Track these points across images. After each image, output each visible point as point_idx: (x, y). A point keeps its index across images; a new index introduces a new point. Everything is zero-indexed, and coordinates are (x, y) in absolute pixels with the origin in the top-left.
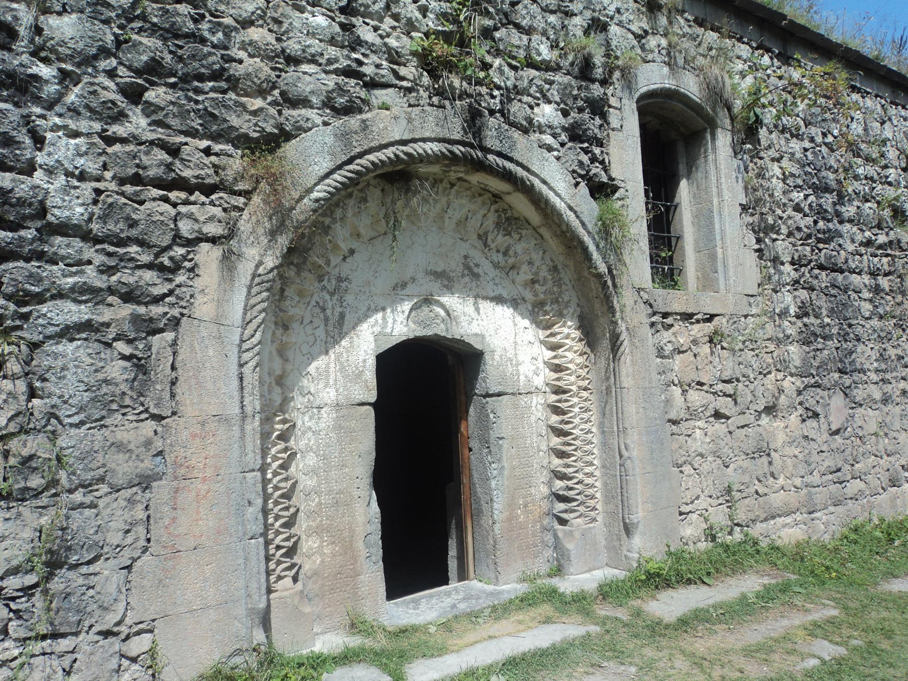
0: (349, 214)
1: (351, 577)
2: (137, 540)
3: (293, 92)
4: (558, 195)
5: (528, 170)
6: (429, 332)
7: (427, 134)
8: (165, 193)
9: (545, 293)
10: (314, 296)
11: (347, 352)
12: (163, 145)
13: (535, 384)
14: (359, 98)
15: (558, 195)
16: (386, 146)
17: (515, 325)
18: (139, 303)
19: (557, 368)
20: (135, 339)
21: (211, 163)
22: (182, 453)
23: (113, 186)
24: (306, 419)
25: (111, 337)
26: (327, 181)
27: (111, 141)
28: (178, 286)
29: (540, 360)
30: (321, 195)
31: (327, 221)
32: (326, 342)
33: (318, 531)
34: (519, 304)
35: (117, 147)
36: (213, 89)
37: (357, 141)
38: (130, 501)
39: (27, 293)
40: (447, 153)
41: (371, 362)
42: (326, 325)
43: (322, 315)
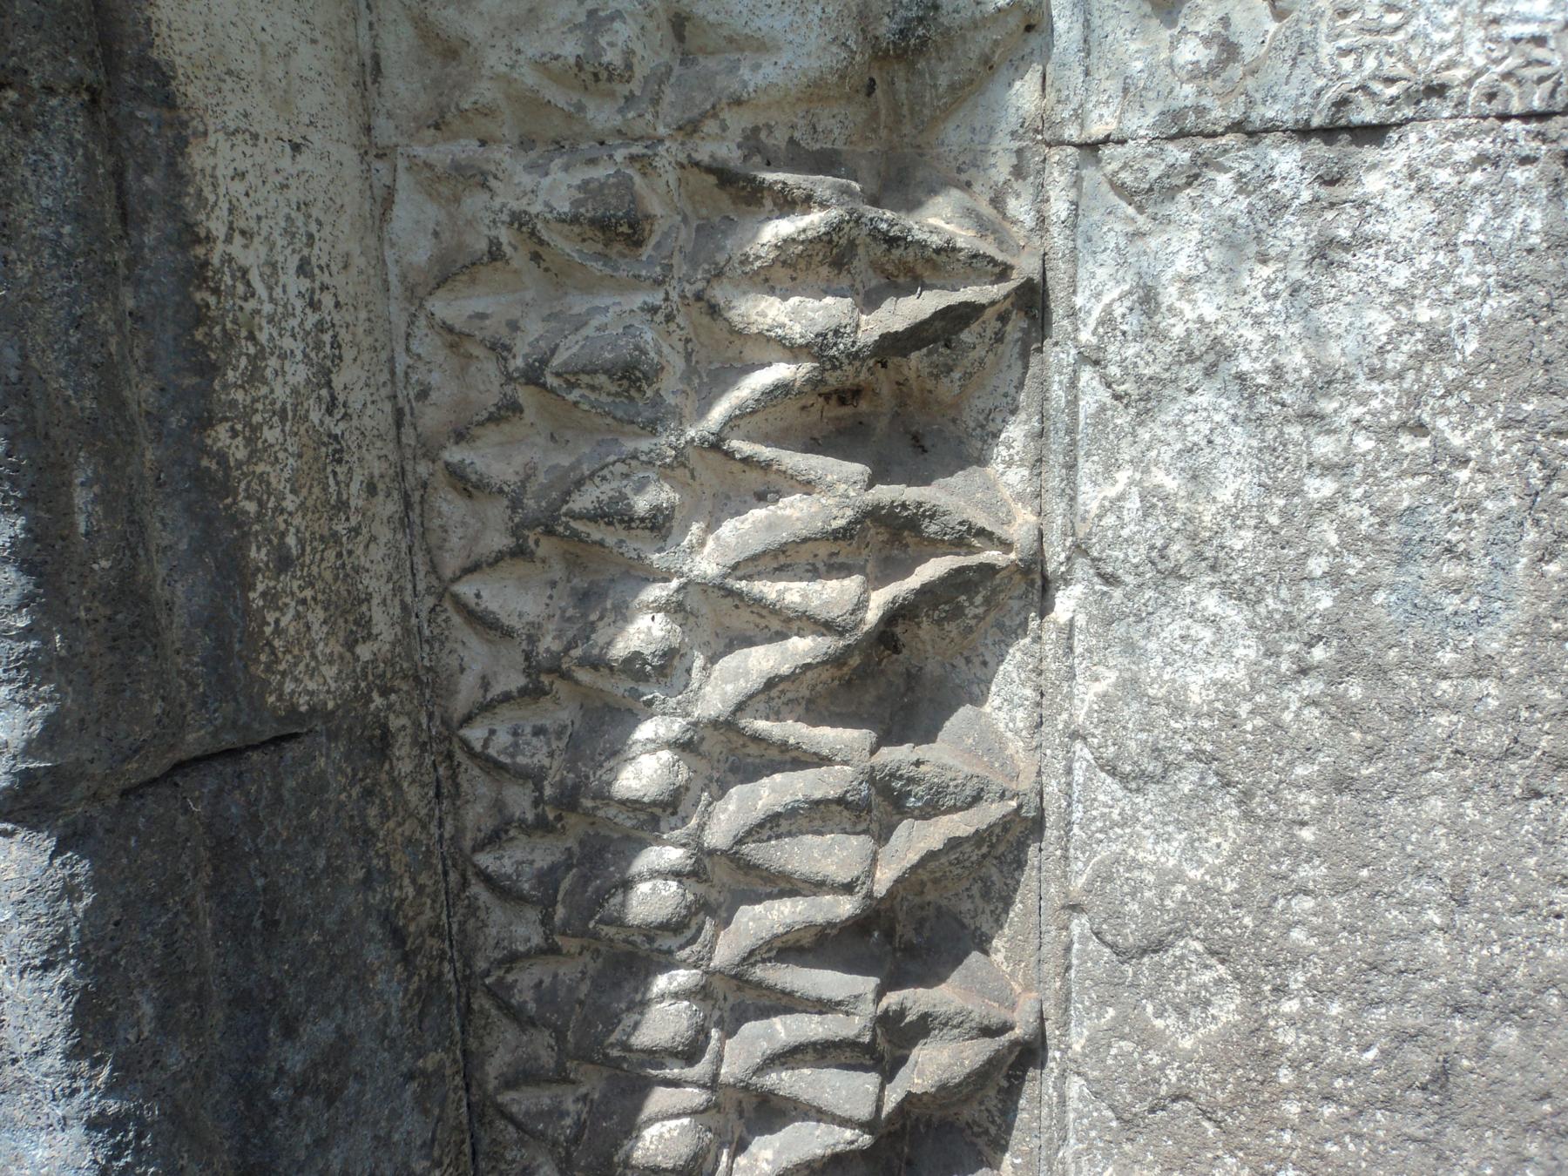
24: (1180, 247)
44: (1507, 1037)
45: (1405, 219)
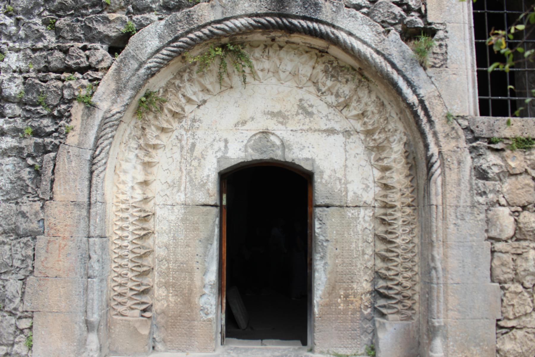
0: (195, 76)
1: (188, 320)
2: (28, 266)
3: (140, 4)
4: (364, 43)
5: (334, 26)
7: (239, 13)
8: (58, 75)
9: (373, 124)
10: (174, 132)
11: (196, 169)
12: (60, 49)
13: (364, 199)
15: (364, 43)
16: (204, 26)
17: (346, 151)
18: (40, 137)
20: (36, 156)
21: (85, 55)
22: (52, 220)
23: (33, 74)
25: (25, 155)
26: (158, 55)
28: (60, 126)
29: (371, 179)
30: (151, 65)
31: (177, 82)
32: (180, 163)
33: (167, 285)
34: (352, 135)
35: (37, 54)
36: (93, 13)
37: (180, 26)
38: (25, 244)
42: (181, 151)
43: (179, 145)
44: (185, 265)
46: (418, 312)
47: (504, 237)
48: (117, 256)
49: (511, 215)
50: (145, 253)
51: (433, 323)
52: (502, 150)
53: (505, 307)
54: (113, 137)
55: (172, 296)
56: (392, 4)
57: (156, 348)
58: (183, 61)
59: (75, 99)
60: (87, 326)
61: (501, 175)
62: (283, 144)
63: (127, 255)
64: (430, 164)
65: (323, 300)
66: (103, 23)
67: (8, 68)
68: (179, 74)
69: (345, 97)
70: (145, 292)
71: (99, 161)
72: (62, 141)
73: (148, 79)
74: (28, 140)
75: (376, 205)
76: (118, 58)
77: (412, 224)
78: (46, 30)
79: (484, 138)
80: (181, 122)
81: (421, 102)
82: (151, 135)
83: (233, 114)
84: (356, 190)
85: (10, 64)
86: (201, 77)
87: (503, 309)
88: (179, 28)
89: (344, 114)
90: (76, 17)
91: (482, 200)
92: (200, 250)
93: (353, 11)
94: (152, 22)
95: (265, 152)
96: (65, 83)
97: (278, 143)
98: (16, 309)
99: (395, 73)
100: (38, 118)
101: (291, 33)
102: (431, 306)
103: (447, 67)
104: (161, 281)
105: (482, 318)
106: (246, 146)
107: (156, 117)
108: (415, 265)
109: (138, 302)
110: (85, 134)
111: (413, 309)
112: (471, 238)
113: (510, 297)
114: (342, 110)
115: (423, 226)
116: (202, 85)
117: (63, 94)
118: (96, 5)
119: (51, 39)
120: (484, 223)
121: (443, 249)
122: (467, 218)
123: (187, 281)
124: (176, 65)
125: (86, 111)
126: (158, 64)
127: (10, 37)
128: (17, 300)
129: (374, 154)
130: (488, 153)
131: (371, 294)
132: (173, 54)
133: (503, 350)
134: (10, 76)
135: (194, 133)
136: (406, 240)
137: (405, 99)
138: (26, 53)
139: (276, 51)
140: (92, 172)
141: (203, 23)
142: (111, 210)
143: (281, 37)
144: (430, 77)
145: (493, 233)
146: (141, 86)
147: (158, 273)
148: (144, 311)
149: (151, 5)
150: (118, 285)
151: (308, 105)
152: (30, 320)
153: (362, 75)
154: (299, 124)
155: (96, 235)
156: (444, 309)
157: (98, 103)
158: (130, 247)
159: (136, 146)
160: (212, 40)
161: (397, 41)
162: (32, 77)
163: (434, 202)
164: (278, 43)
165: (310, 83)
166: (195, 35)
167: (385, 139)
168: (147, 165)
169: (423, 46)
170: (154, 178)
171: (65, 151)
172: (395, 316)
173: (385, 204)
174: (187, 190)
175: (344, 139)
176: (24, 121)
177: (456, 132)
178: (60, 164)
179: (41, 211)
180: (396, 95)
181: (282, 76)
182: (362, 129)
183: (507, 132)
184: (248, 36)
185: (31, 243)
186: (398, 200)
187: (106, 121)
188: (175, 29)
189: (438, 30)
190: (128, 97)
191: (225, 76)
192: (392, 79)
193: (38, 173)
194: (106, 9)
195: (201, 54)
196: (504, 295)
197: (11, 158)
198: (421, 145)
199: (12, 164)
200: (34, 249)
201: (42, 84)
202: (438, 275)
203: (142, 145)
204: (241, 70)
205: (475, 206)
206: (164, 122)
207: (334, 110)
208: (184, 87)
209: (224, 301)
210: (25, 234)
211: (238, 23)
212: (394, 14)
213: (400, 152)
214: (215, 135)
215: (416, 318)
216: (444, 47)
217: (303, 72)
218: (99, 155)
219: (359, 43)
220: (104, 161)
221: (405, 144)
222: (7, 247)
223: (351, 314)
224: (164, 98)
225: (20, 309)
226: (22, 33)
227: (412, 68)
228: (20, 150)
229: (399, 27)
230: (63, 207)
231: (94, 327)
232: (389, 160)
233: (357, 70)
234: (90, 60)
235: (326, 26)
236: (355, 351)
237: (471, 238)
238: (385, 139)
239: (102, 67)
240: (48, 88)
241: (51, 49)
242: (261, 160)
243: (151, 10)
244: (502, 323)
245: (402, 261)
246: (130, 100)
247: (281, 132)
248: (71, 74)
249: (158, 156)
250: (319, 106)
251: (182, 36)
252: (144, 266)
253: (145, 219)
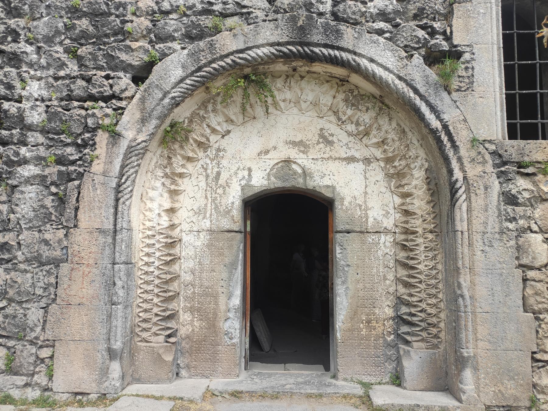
0: (219, 107)
1: (212, 345)
2: (50, 294)
5: (355, 53)
6: (287, 185)
7: (261, 42)
8: (81, 103)
9: (394, 151)
11: (221, 196)
12: (83, 78)
13: (385, 225)
14: (207, 27)
16: (227, 56)
17: (366, 178)
18: (64, 165)
19: (407, 213)
20: (60, 184)
21: (109, 83)
22: (76, 248)
23: (55, 103)
25: (48, 183)
26: (182, 85)
27: (57, 79)
28: (85, 155)
30: (176, 94)
31: (202, 112)
33: (192, 310)
34: (372, 162)
35: (60, 82)
36: (115, 41)
37: (203, 56)
38: (48, 272)
39: (13, 161)
40: (275, 52)
41: (238, 203)
42: (207, 180)
43: (204, 174)
44: (210, 290)
45: (202, 237)
46: (444, 341)
47: (537, 264)
48: (143, 281)
49: (544, 242)
50: (171, 278)
51: (462, 353)
52: (534, 174)
53: (541, 339)
54: (139, 165)
55: (197, 321)
56: (416, 28)
57: (180, 375)
58: (207, 91)
59: (99, 128)
60: (110, 354)
61: (532, 201)
62: (304, 172)
63: (153, 281)
64: (454, 190)
65: (345, 325)
66: (125, 52)
67: (30, 97)
68: (204, 105)
69: (365, 126)
70: (170, 317)
71: (125, 189)
72: (86, 169)
73: (172, 108)
74: (52, 168)
75: (397, 231)
76: (142, 88)
77: (434, 250)
78: (68, 58)
79: (514, 162)
80: (206, 152)
81: (445, 127)
82: (177, 164)
83: (256, 144)
84: (375, 215)
85: (31, 92)
86: (224, 107)
87: (538, 341)
88: (202, 58)
89: (364, 142)
90: (98, 45)
91: (511, 226)
92: (225, 275)
93: (375, 37)
94: (175, 51)
95: (287, 180)
96: (88, 112)
97: (300, 171)
98: (37, 338)
99: (418, 98)
100: (61, 146)
101: (312, 62)
102: (458, 335)
103: (473, 91)
104: (187, 306)
105: (516, 350)
106: (269, 174)
107: (182, 147)
108: (439, 292)
109: (163, 327)
110: (111, 162)
111: (439, 338)
112: (500, 266)
113: (546, 329)
114: (362, 138)
115: (447, 253)
116: (226, 116)
117: (86, 123)
118: (118, 34)
119: (73, 68)
120: (514, 250)
121: (470, 276)
122: (496, 244)
123: (212, 306)
124: (200, 95)
125: (111, 139)
126: (182, 94)
127: (31, 65)
128: (38, 329)
129: (394, 180)
130: (518, 177)
131: (393, 320)
132: (197, 84)
133: (541, 386)
134: (32, 104)
135: (219, 162)
136: (429, 266)
137: (427, 125)
138: (48, 82)
139: (297, 82)
140: (117, 200)
141: (226, 52)
142: (138, 237)
143: (302, 67)
144: (455, 102)
145: (525, 261)
146: (166, 116)
147: (183, 298)
148: (169, 336)
149: (173, 34)
150: (143, 311)
151: (329, 134)
152: (51, 349)
153: (383, 103)
154: (320, 153)
155: (121, 262)
156: (473, 339)
157: (123, 132)
158: (157, 273)
159: (162, 175)
160: (235, 71)
161: (420, 66)
162: (54, 106)
163: (459, 227)
164: (300, 73)
165: (330, 113)
166: (218, 65)
167: (406, 166)
168: (174, 193)
169: (448, 70)
170: (180, 205)
171: (90, 179)
172: (420, 344)
173: (406, 230)
174: (213, 217)
175: (364, 166)
176: (47, 149)
177: (483, 157)
178: (84, 192)
179: (64, 239)
180: (418, 121)
181: (304, 106)
182: (382, 156)
183: (539, 157)
184: (270, 66)
185: (54, 271)
186: (419, 226)
187: (131, 150)
188: (198, 58)
189: (464, 52)
190: (153, 127)
191: (248, 107)
192: (415, 104)
193: (62, 200)
194: (128, 37)
195: (225, 85)
196: (540, 326)
197: (34, 186)
198: (444, 171)
199: (35, 192)
200: (57, 277)
201: (65, 112)
202: (465, 304)
203: (169, 174)
204: (263, 100)
205: (505, 233)
206: (189, 151)
207: (354, 138)
208: (208, 118)
209: (248, 325)
210: (48, 262)
211: (260, 52)
212: (418, 37)
213: (421, 178)
214: (239, 164)
215: (442, 347)
216: (470, 70)
217: (323, 102)
218: (125, 183)
219: (380, 69)
220: (129, 189)
221: (427, 170)
222: (29, 275)
223: (374, 340)
224: (189, 128)
225: (42, 338)
226: (43, 61)
227: (435, 93)
228: (43, 178)
229: (423, 51)
230: (88, 234)
231: (117, 355)
232: (410, 187)
233: (378, 97)
234: (113, 89)
235: (347, 53)
236: (379, 379)
237: (500, 266)
238: (406, 166)
239: (126, 96)
240: (72, 116)
241: (74, 78)
242: (283, 187)
243: (174, 39)
244: (538, 356)
245: (426, 287)
246: (155, 130)
247: (303, 160)
248: (94, 103)
249: (185, 184)
250: (340, 135)
251: (205, 65)
252: (170, 291)
253: (172, 245)
